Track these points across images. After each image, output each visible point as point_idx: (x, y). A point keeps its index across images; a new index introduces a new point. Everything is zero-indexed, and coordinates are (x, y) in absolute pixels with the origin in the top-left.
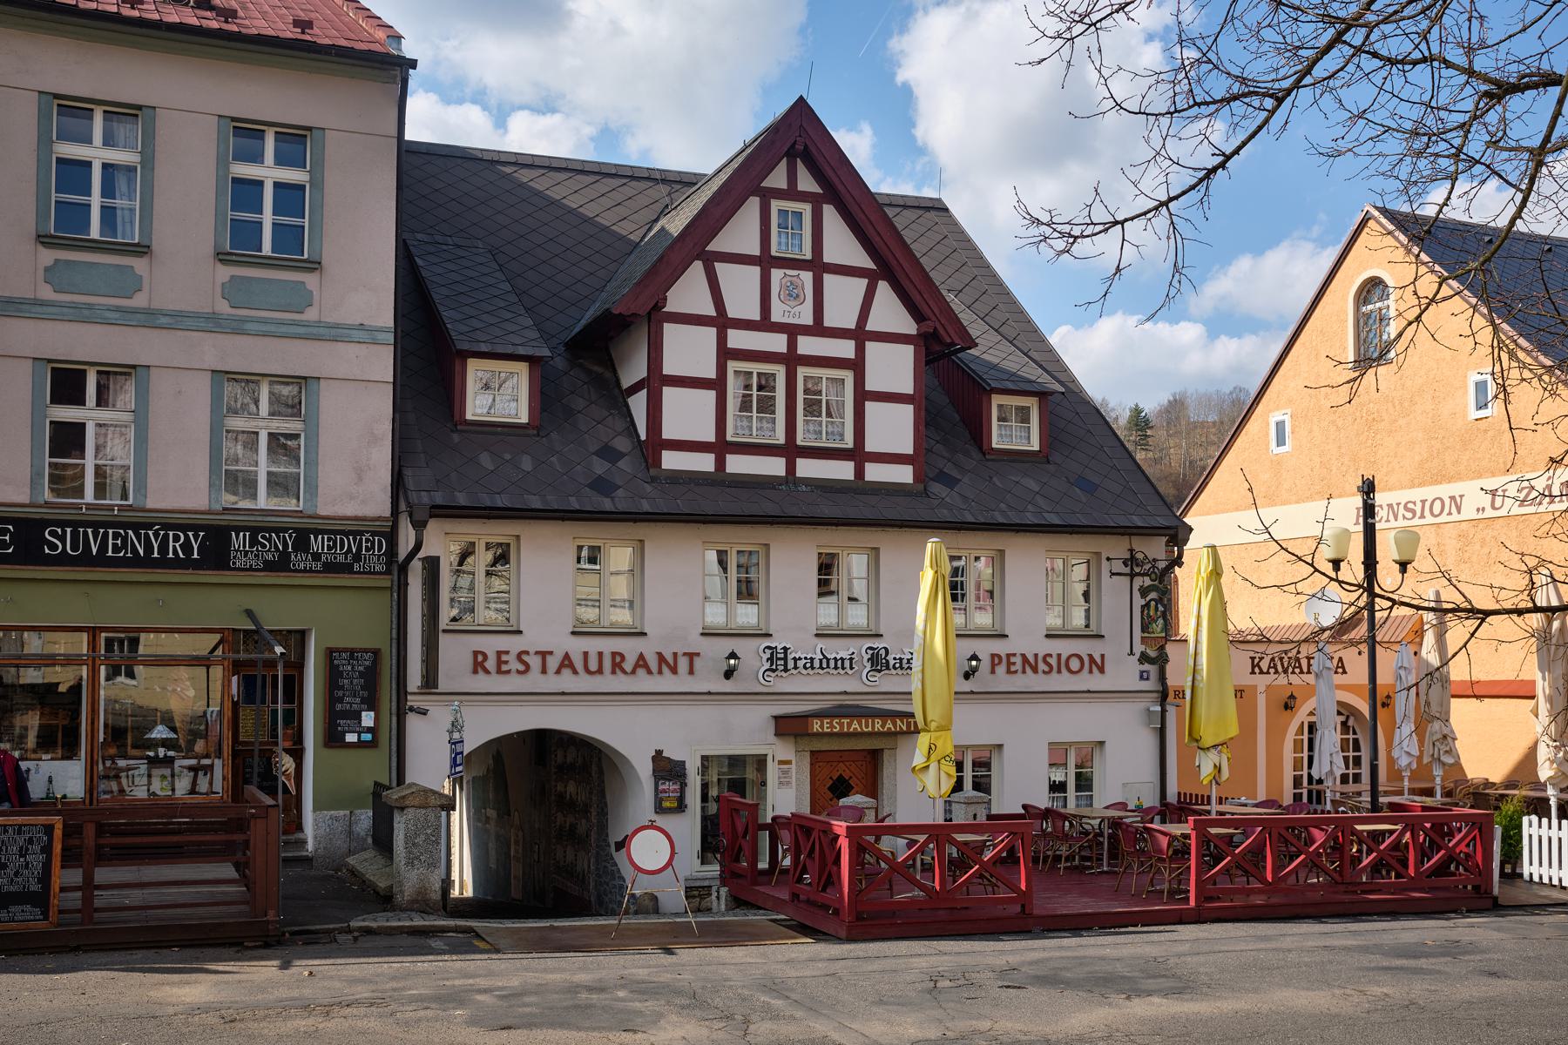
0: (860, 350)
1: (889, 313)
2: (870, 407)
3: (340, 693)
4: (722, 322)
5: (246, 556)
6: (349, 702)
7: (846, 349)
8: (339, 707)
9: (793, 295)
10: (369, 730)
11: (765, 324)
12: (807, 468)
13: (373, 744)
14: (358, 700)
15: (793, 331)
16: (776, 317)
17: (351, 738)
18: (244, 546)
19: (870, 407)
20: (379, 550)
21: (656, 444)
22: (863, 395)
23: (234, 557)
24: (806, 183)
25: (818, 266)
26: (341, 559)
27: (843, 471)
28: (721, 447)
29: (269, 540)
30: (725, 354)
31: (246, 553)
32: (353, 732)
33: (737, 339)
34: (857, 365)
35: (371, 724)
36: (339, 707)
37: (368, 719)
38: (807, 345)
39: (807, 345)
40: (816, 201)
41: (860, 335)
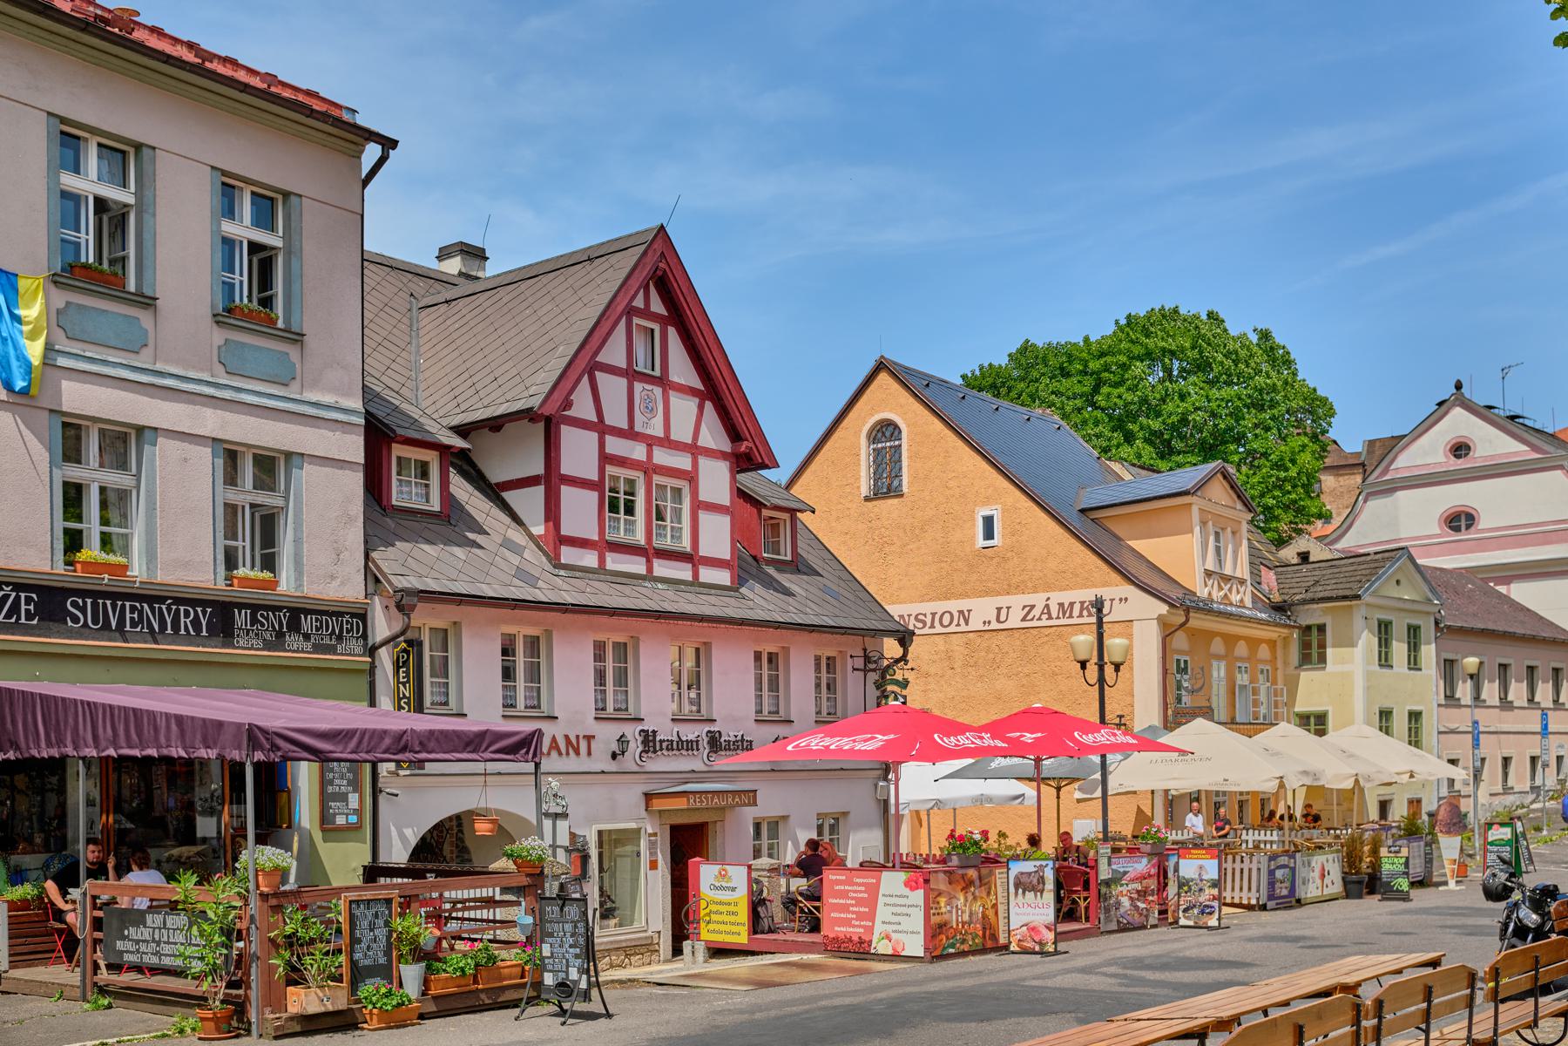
0: (695, 464)
2: (703, 516)
3: (331, 775)
5: (247, 635)
7: (683, 462)
11: (630, 434)
14: (345, 782)
15: (651, 442)
16: (638, 428)
18: (246, 625)
19: (703, 516)
20: (358, 633)
22: (698, 506)
23: (238, 636)
24: (657, 306)
26: (327, 641)
29: (267, 619)
30: (605, 459)
31: (248, 631)
32: (343, 814)
33: (615, 446)
34: (692, 477)
37: (353, 801)
38: (662, 457)
39: (662, 457)
40: (663, 321)
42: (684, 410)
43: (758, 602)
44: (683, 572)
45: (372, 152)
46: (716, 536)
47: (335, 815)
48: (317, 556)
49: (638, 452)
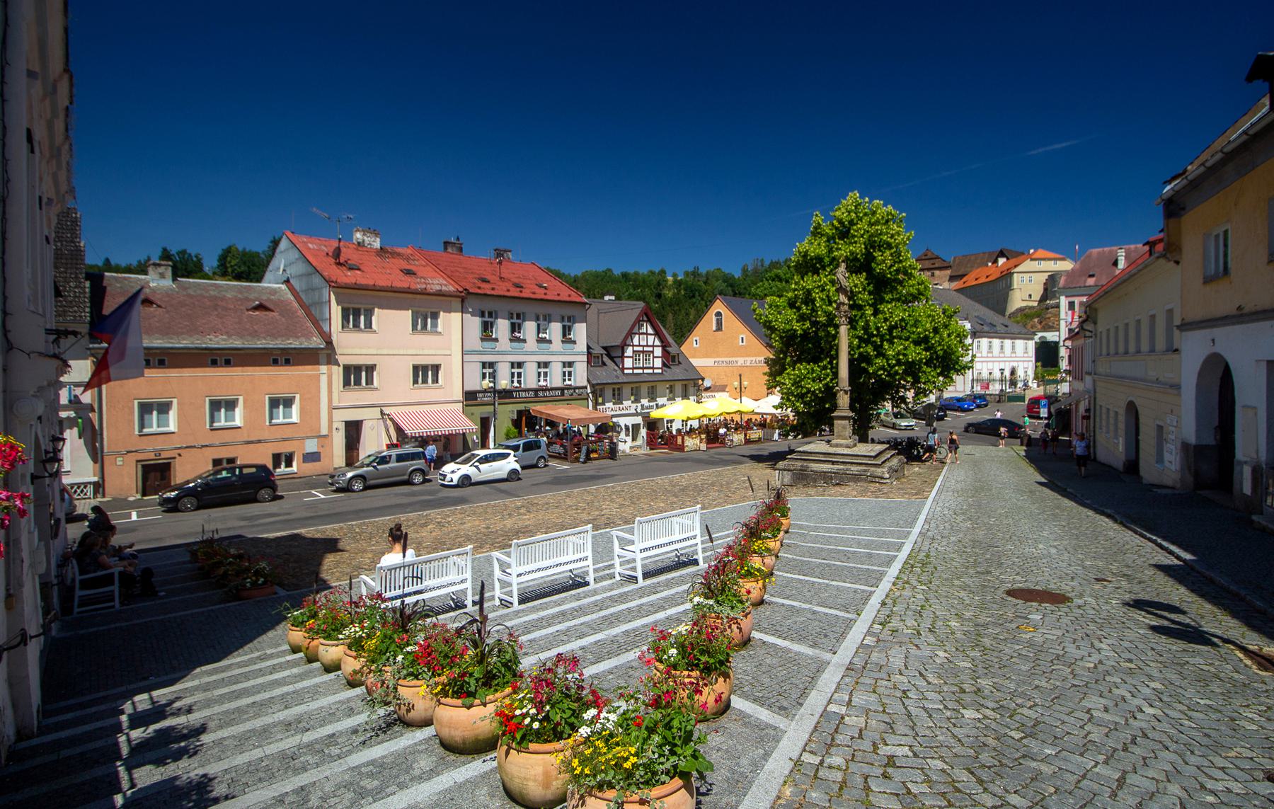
1: (657, 342)
4: (633, 346)
9: (643, 340)
11: (639, 346)
12: (646, 371)
15: (643, 346)
21: (623, 369)
22: (654, 357)
25: (647, 334)
27: (651, 371)
28: (633, 368)
30: (634, 351)
33: (636, 349)
34: (653, 352)
39: (646, 349)
41: (653, 346)
42: (651, 338)
43: (669, 375)
44: (651, 371)
45: (587, 306)
46: (658, 363)
48: (578, 379)
49: (641, 349)
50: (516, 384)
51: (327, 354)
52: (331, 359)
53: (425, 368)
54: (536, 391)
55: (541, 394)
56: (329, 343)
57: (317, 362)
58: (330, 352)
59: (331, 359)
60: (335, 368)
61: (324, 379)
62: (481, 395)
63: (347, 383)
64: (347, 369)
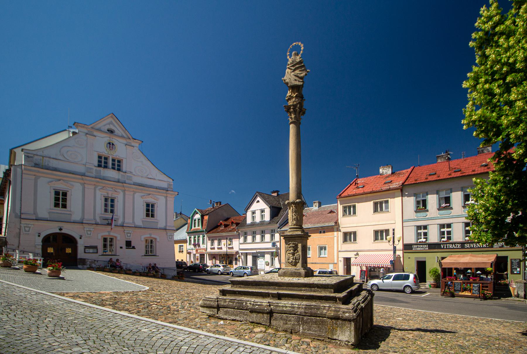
6: (515, 267)
8: (513, 268)
10: (519, 271)
13: (520, 274)
17: (515, 272)
35: (519, 270)
36: (513, 268)
37: (518, 269)
47: (514, 272)
50: (445, 239)
51: (336, 227)
52: (338, 230)
53: (382, 232)
54: (462, 244)
55: (467, 246)
56: (336, 223)
57: (333, 231)
58: (337, 227)
59: (338, 230)
60: (339, 233)
61: (336, 238)
62: (415, 246)
63: (345, 240)
64: (346, 234)
